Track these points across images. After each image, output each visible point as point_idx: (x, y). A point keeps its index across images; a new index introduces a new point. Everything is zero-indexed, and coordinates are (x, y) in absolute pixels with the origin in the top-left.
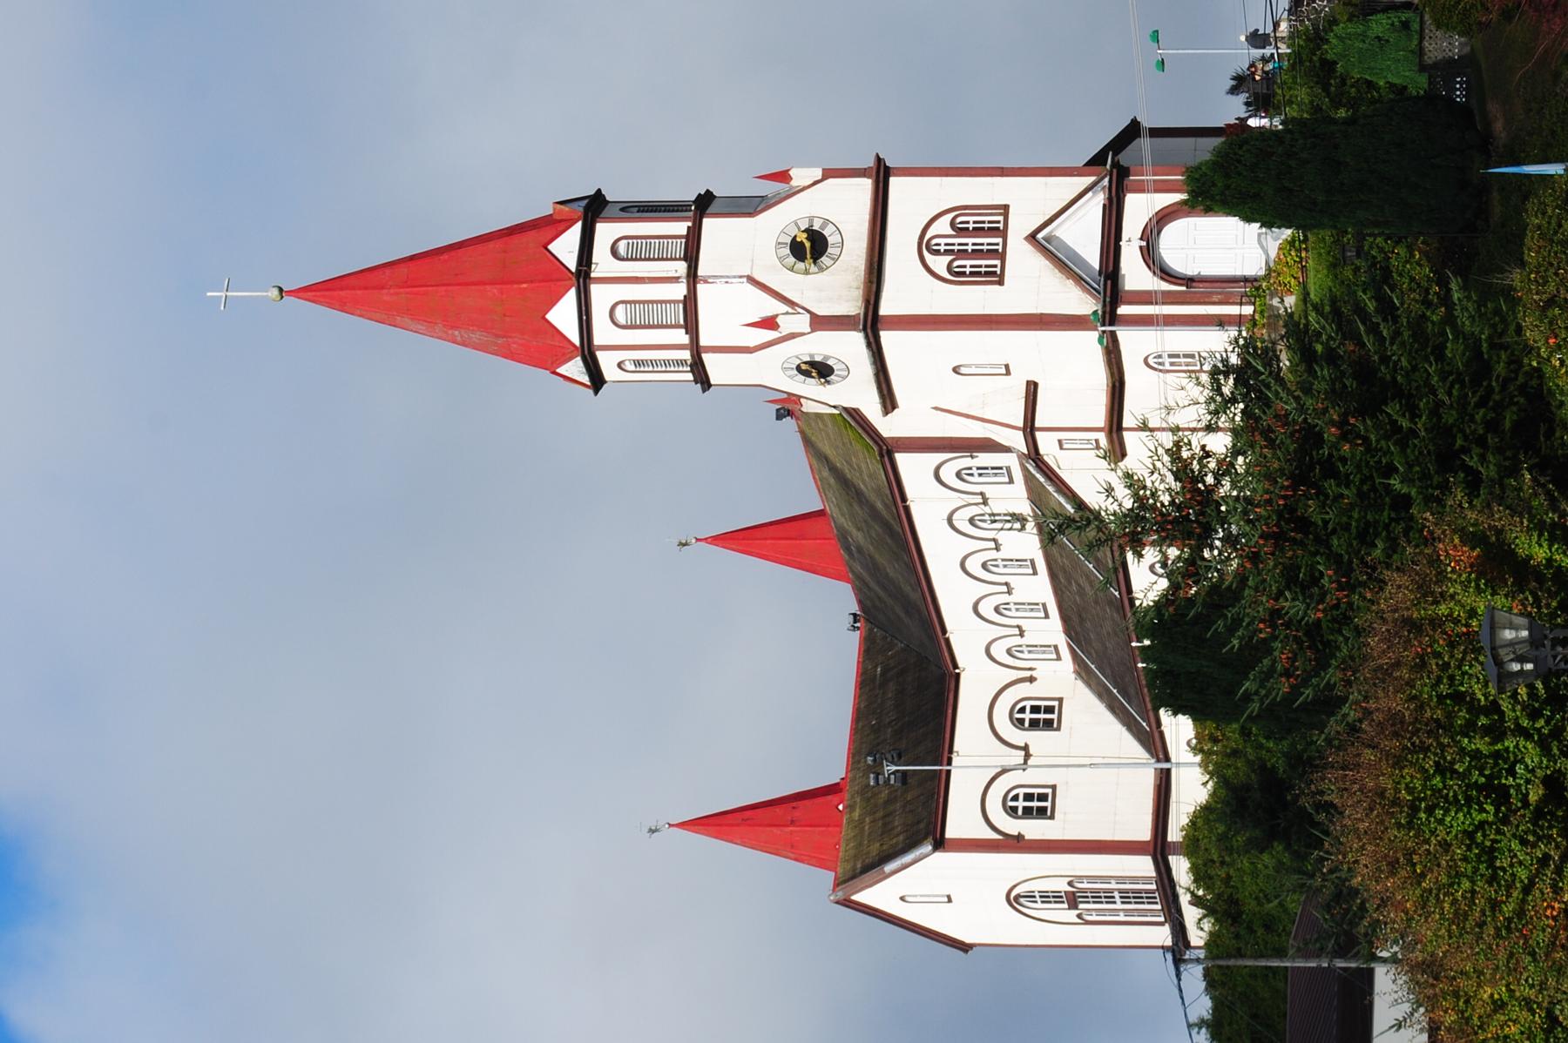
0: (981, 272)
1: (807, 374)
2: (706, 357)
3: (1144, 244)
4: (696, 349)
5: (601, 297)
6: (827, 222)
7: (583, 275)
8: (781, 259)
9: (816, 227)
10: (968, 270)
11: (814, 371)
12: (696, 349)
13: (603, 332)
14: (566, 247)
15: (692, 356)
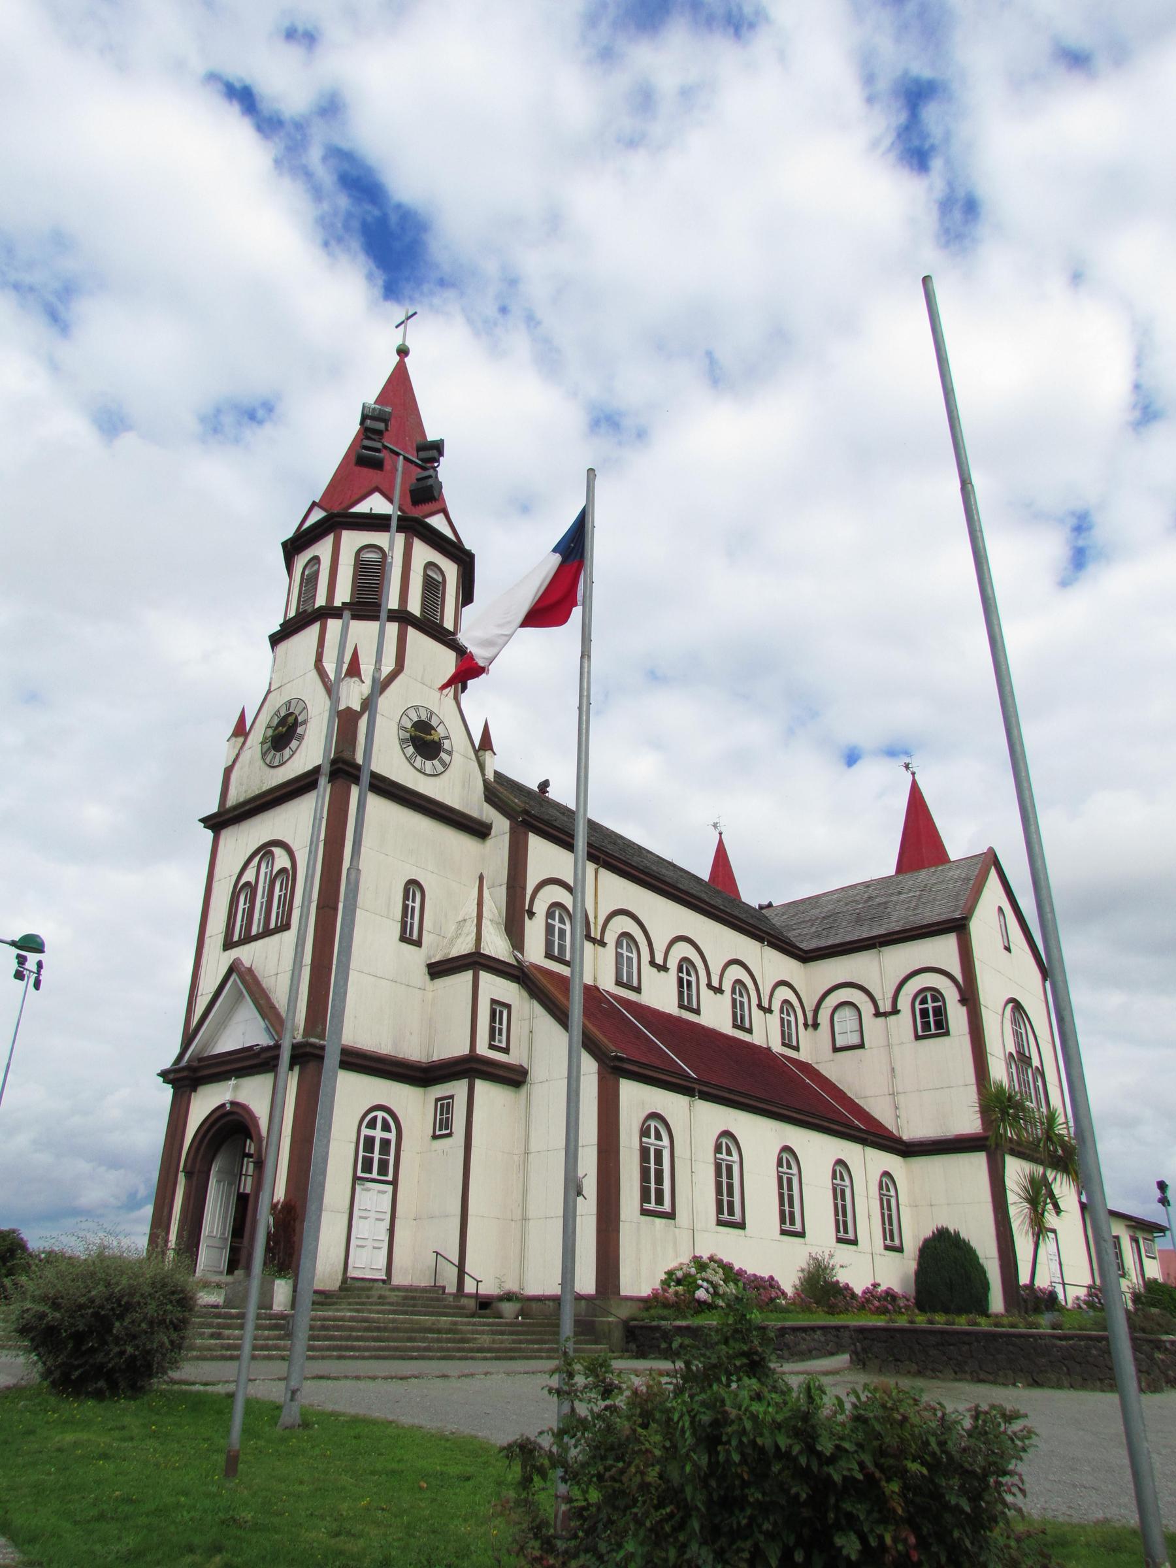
0: (407, 918)
1: (283, 721)
2: (316, 627)
3: (228, 1107)
4: (329, 612)
5: (392, 542)
6: (446, 766)
7: (413, 527)
8: (416, 708)
9: (443, 755)
10: (410, 903)
11: (284, 729)
12: (329, 612)
13: (352, 540)
14: (437, 522)
15: (321, 607)
